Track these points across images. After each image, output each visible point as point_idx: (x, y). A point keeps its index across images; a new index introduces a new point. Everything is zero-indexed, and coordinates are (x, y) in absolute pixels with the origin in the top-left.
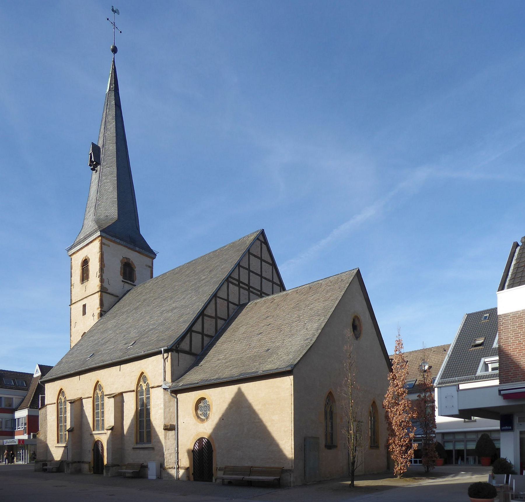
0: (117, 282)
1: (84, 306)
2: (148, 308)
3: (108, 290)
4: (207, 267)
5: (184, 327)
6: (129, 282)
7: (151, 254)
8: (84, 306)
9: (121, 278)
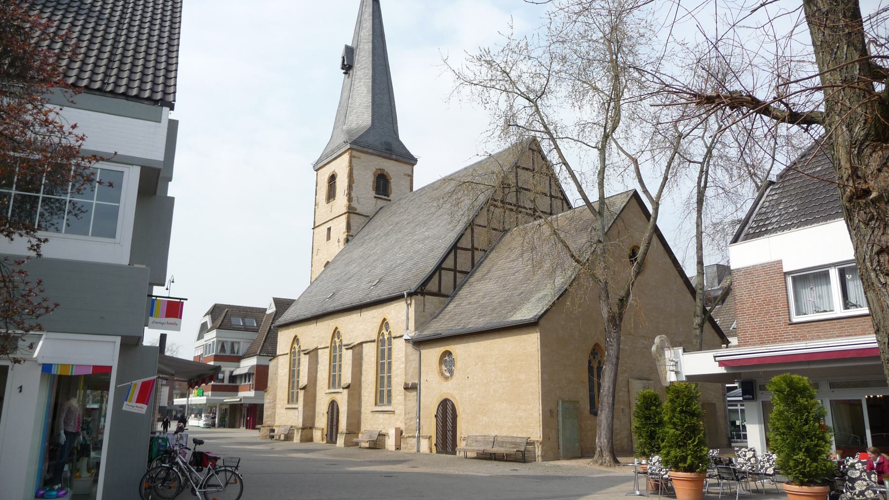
0: (367, 198)
1: (329, 229)
2: (400, 235)
7: (411, 160)
8: (329, 229)
9: (373, 193)
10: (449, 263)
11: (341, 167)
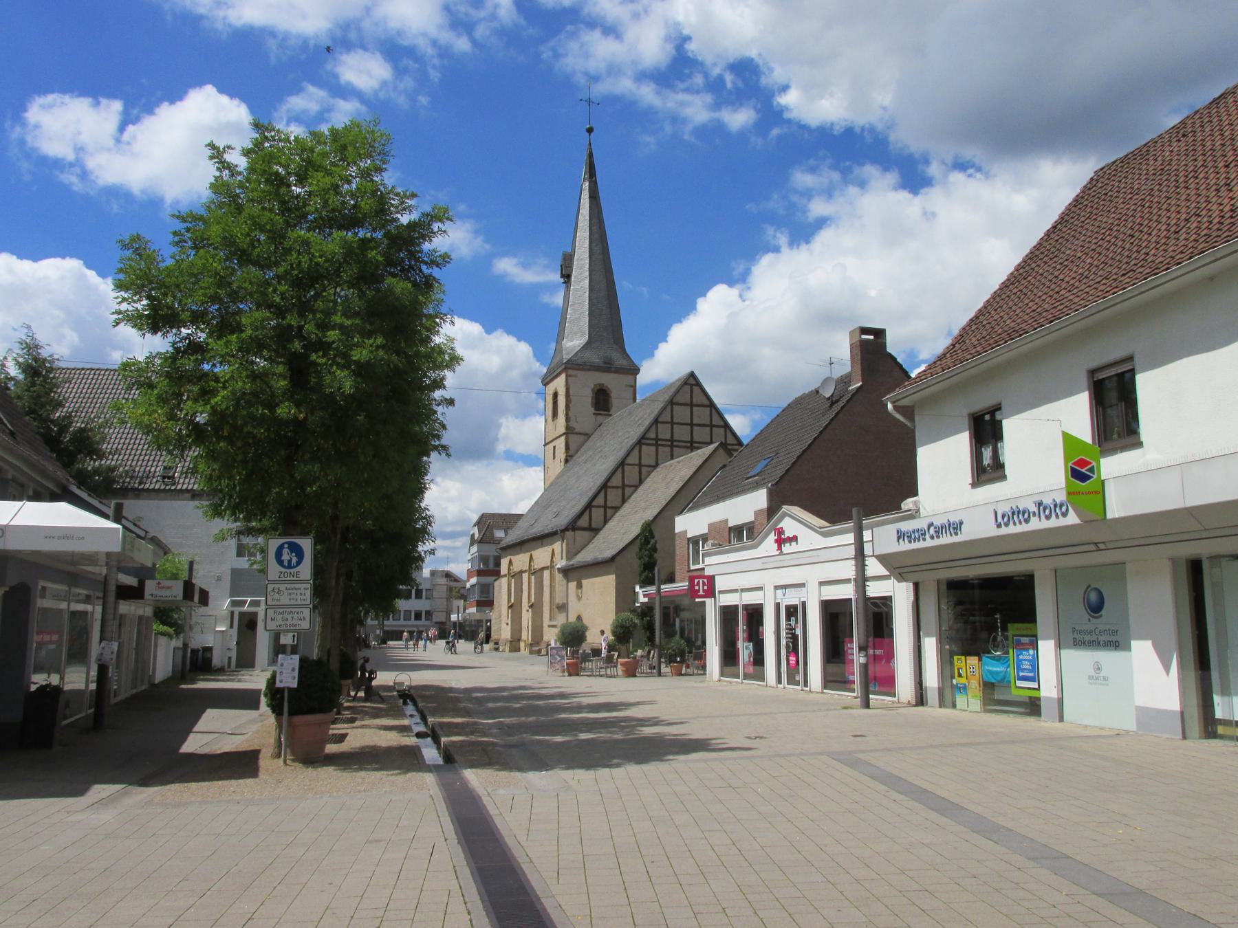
5: (584, 500)
9: (592, 410)
11: (560, 384)
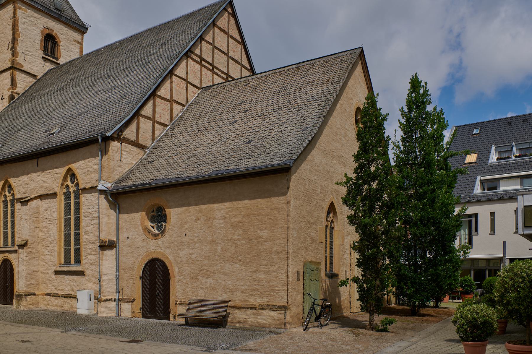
2: (76, 89)
3: (23, 67)
4: (158, 40)
6: (51, 59)
9: (41, 53)
10: (147, 110)
